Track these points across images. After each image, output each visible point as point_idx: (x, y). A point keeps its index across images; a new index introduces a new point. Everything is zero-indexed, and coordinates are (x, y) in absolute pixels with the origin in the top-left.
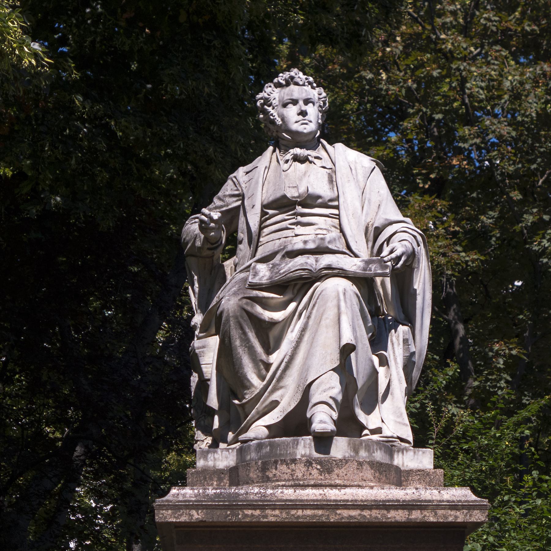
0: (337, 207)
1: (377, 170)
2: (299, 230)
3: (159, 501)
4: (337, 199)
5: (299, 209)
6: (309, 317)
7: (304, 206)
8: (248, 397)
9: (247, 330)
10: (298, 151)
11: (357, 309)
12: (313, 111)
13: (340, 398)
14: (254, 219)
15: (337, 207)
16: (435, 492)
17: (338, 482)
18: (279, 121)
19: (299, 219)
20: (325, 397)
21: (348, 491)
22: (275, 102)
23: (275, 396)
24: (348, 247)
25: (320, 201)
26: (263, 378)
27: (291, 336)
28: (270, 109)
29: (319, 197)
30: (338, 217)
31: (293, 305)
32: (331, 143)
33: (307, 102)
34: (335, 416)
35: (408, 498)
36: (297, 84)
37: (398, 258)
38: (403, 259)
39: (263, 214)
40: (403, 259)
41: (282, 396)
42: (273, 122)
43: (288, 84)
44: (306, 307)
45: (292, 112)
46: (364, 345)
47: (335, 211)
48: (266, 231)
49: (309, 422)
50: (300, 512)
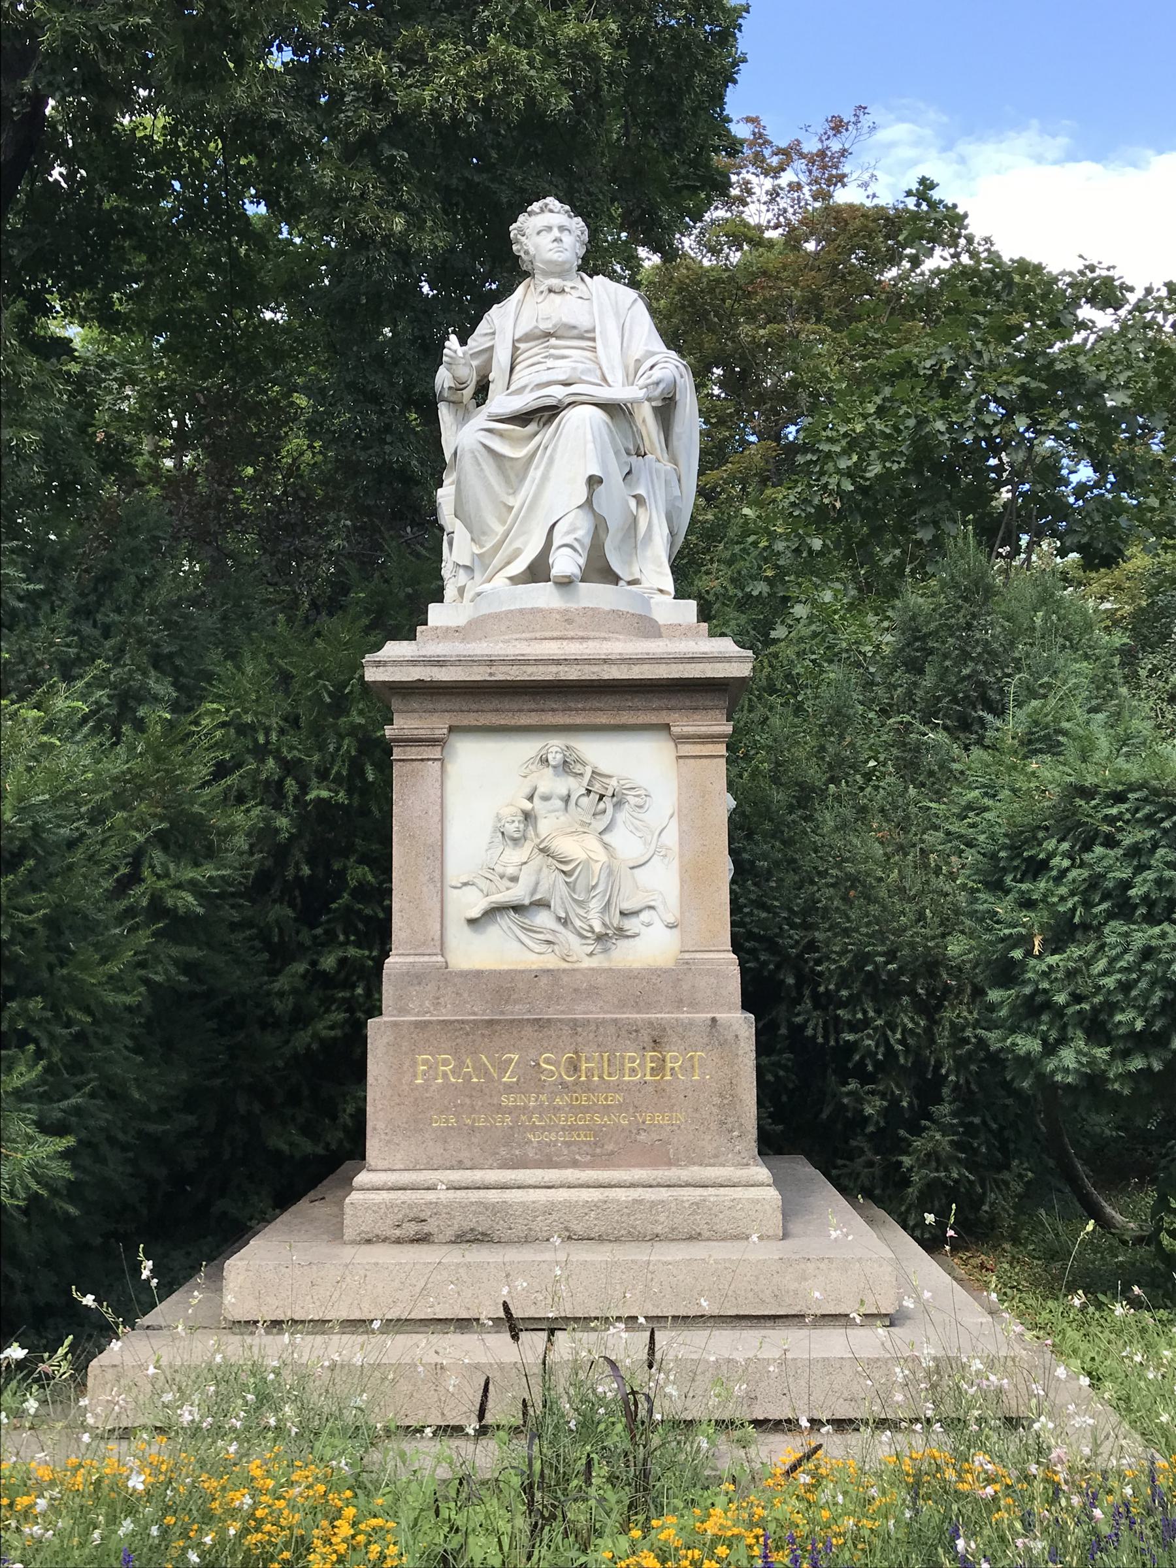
0: (593, 340)
1: (640, 302)
2: (550, 363)
3: (368, 657)
4: (593, 330)
5: (553, 341)
6: (554, 450)
7: (557, 338)
8: (488, 546)
9: (484, 466)
10: (555, 282)
11: (607, 438)
12: (568, 239)
13: (587, 541)
14: (502, 357)
15: (593, 340)
16: (692, 643)
17: (581, 634)
18: (532, 251)
19: (552, 351)
20: (568, 540)
21: (591, 643)
22: (527, 232)
23: (517, 544)
24: (605, 379)
25: (575, 332)
26: (504, 523)
27: (535, 474)
28: (523, 239)
29: (574, 327)
30: (594, 349)
31: (538, 438)
32: (591, 276)
33: (562, 229)
34: (582, 561)
35: (660, 650)
36: (551, 211)
37: (657, 384)
38: (662, 386)
39: (515, 349)
40: (662, 386)
41: (526, 544)
42: (527, 253)
43: (542, 211)
44: (551, 440)
45: (545, 240)
46: (615, 476)
47: (591, 344)
48: (518, 368)
49: (548, 568)
50: (530, 669)
